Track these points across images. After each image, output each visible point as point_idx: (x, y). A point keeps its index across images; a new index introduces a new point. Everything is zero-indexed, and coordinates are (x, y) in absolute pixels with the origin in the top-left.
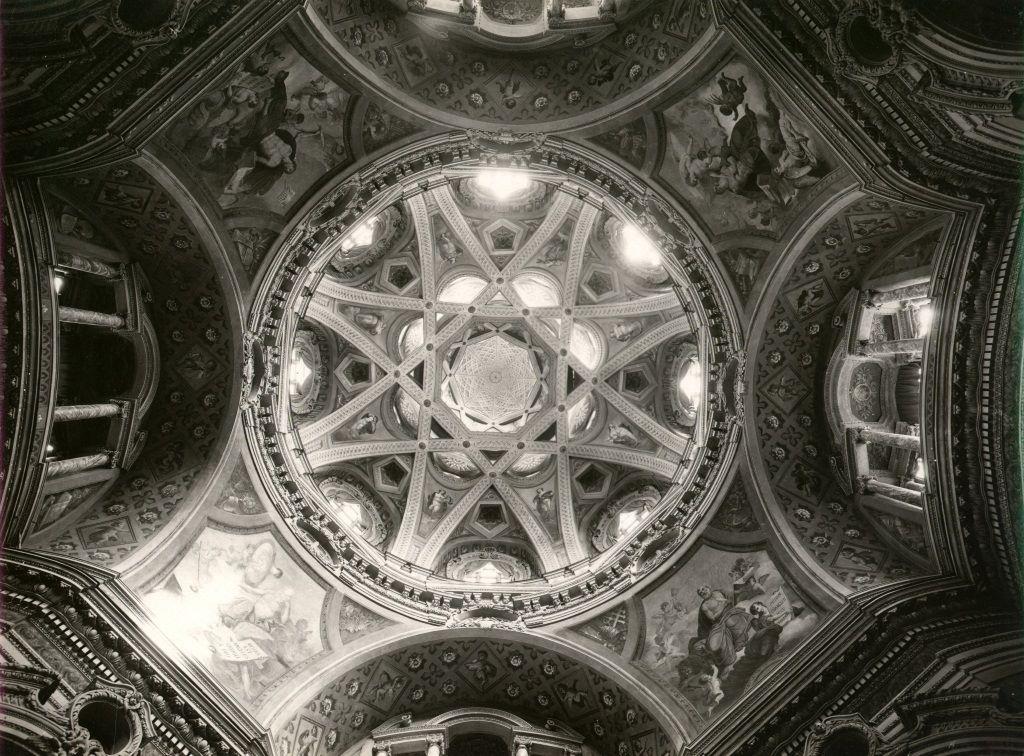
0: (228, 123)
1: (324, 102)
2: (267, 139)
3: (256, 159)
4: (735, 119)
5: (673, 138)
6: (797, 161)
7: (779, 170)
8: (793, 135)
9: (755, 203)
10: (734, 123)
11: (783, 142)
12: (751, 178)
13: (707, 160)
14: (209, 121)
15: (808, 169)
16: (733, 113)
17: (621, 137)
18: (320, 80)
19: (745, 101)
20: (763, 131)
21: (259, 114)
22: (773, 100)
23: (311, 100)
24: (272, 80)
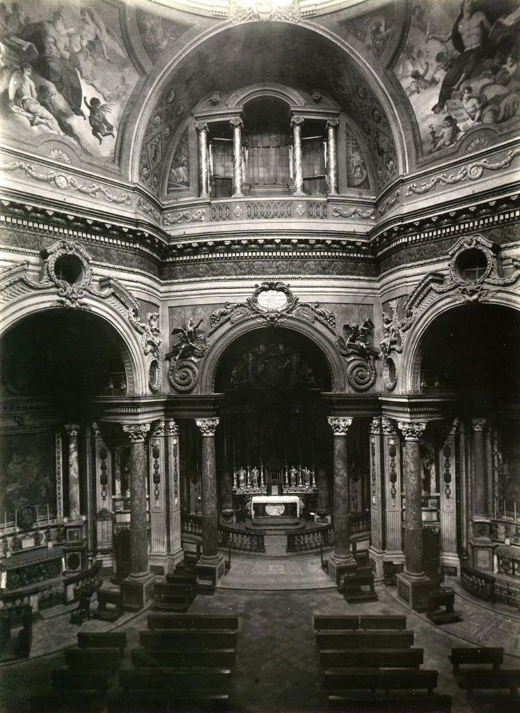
0: (494, 83)
1: (416, 69)
2: (474, 47)
3: (491, 29)
4: (85, 98)
5: (121, 52)
6: (23, 95)
7: (27, 73)
8: (41, 117)
9: (23, 23)
10: (84, 94)
11: (43, 104)
12: (42, 48)
13: (85, 43)
14: (505, 96)
15: (11, 95)
16: (89, 104)
17: (165, 37)
18: (412, 93)
19: (88, 120)
20: (60, 101)
21: (468, 78)
22: (72, 140)
23: (425, 74)
24: (445, 107)
